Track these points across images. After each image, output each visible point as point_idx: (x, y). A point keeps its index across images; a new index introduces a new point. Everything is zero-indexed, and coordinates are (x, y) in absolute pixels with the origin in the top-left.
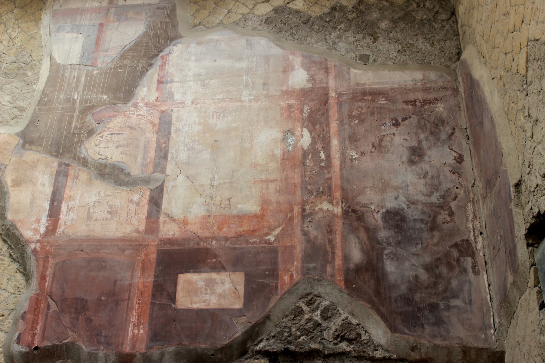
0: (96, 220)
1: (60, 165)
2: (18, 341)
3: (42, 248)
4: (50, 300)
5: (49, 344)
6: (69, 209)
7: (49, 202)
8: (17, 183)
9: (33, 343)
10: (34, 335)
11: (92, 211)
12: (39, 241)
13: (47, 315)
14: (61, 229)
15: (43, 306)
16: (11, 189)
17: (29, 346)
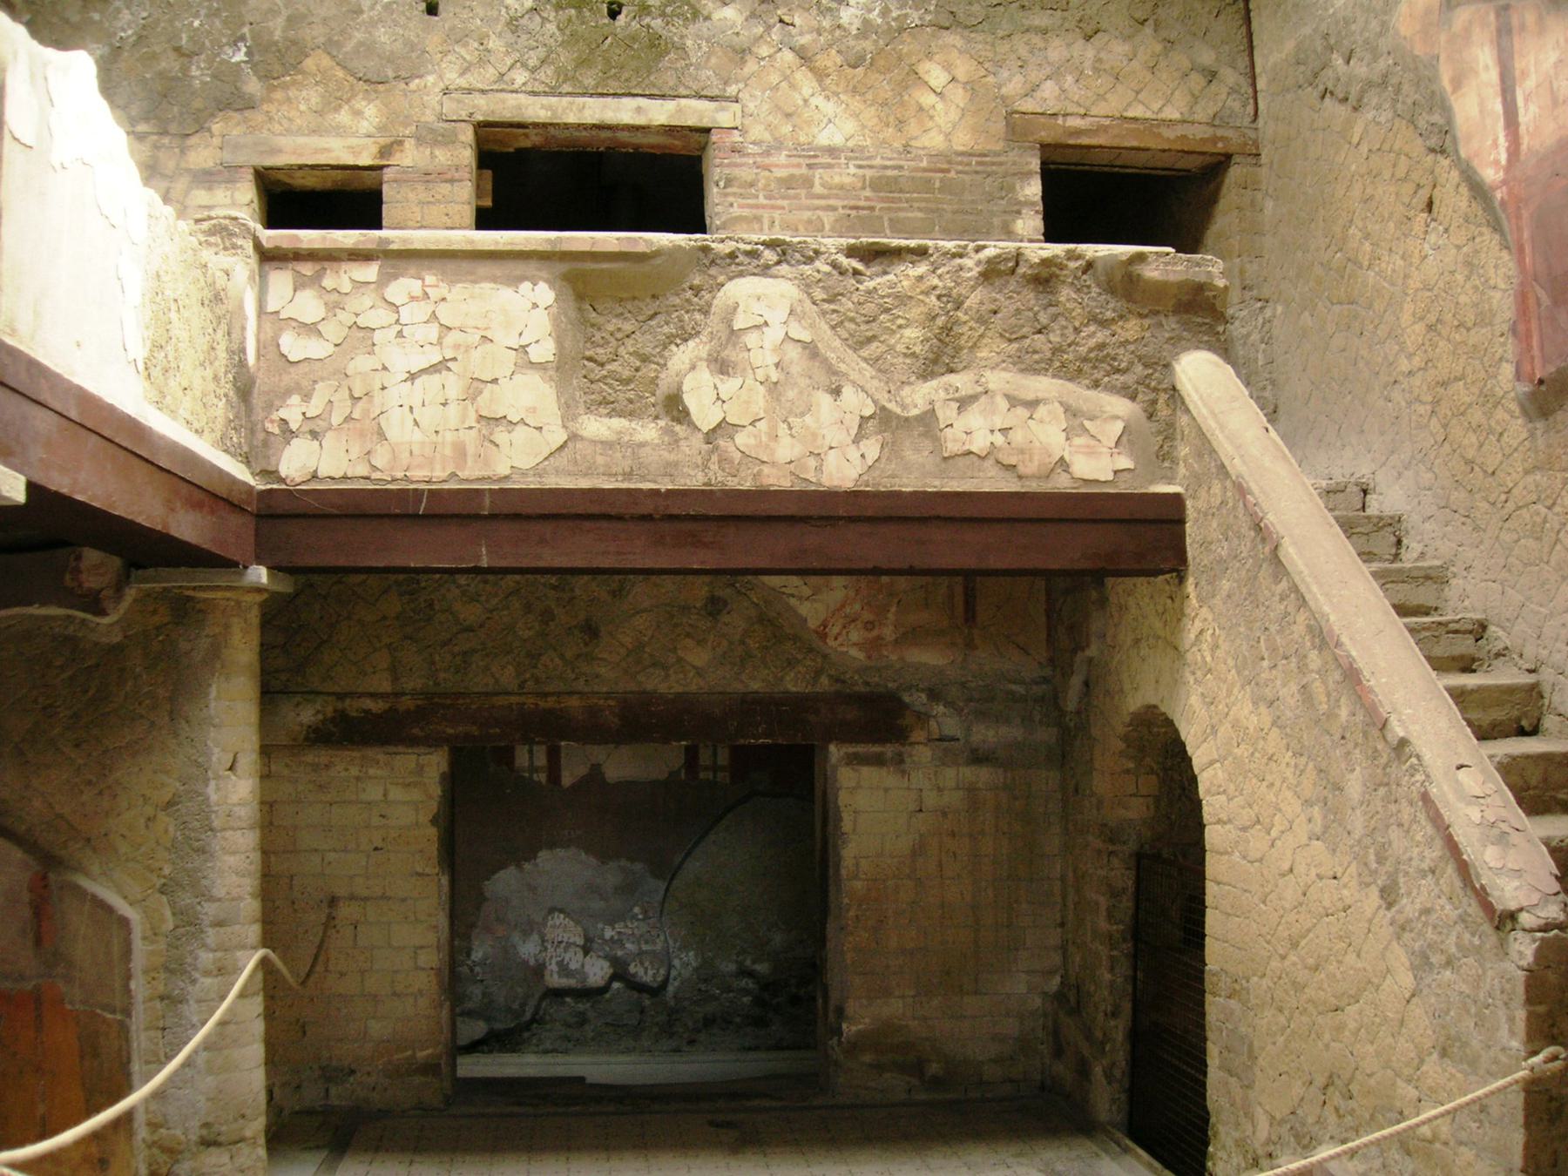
0: (1564, 102)
1: (1498, 16)
2: (1518, 376)
3: (1510, 193)
4: (1537, 288)
5: (1553, 369)
6: (1526, 100)
7: (1499, 100)
8: (1457, 83)
9: (1534, 373)
10: (1532, 358)
11: (1555, 86)
12: (1504, 182)
13: (1539, 319)
14: (1524, 147)
15: (1532, 302)
16: (1452, 98)
17: (1531, 381)
